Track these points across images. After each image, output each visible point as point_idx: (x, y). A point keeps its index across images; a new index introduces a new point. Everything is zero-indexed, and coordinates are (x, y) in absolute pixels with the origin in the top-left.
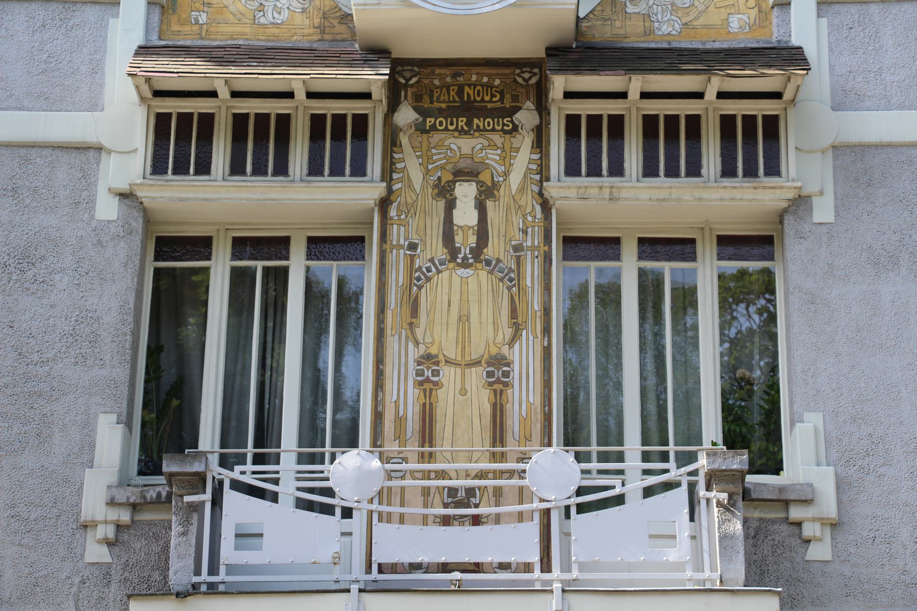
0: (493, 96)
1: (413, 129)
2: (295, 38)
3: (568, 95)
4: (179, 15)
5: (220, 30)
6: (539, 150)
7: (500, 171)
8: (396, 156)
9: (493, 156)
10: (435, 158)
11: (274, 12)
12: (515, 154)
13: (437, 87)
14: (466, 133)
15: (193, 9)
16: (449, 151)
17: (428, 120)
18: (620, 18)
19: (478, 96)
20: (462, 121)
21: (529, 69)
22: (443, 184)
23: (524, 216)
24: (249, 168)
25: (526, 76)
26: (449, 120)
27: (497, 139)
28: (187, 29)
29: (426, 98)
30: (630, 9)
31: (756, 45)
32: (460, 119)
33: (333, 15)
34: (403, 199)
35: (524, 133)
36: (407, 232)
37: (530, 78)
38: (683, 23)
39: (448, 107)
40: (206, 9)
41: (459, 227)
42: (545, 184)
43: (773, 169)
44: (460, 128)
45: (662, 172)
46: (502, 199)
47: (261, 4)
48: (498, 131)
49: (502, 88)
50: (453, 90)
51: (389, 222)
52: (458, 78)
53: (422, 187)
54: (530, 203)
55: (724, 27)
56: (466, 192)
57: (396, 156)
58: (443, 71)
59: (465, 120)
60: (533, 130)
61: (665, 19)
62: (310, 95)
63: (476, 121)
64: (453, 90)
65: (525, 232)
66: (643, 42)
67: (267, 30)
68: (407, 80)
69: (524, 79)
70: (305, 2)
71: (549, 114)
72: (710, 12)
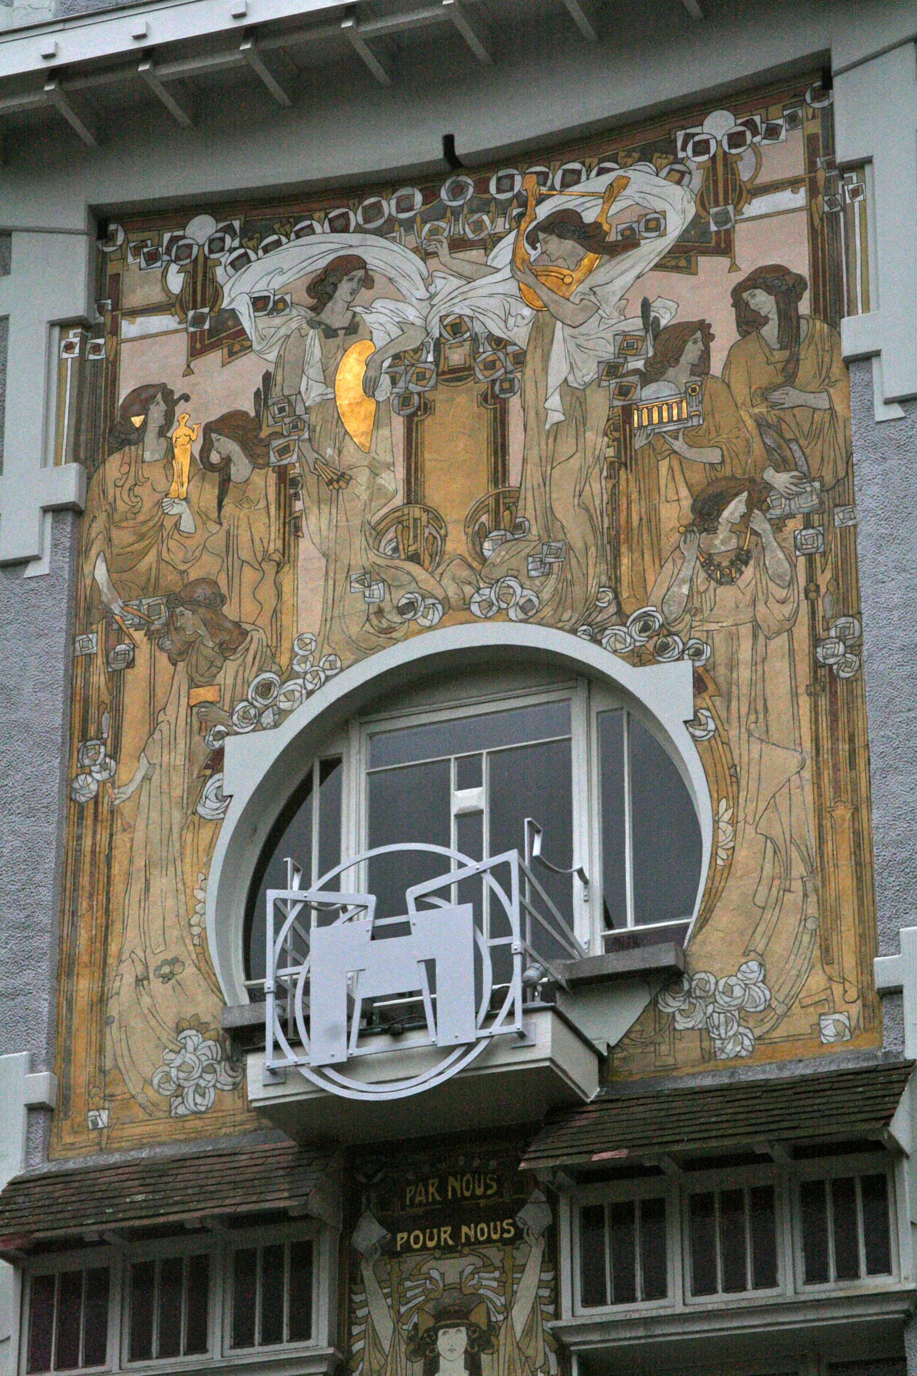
0: (487, 1187)
1: (379, 1253)
2: (224, 1130)
6: (551, 1266)
7: (499, 1304)
8: (357, 1298)
11: (197, 1096)
12: (519, 1275)
15: (91, 1107)
17: (399, 1236)
19: (468, 1189)
20: (445, 1232)
22: (420, 1335)
24: (155, 1348)
28: (82, 1138)
30: (681, 1024)
32: (443, 1229)
34: (366, 1367)
35: (531, 1239)
40: (107, 1105)
46: (502, 1349)
47: (179, 1086)
48: (497, 1241)
59: (449, 1229)
60: (543, 1235)
61: (731, 1033)
63: (465, 1229)
67: (187, 1125)
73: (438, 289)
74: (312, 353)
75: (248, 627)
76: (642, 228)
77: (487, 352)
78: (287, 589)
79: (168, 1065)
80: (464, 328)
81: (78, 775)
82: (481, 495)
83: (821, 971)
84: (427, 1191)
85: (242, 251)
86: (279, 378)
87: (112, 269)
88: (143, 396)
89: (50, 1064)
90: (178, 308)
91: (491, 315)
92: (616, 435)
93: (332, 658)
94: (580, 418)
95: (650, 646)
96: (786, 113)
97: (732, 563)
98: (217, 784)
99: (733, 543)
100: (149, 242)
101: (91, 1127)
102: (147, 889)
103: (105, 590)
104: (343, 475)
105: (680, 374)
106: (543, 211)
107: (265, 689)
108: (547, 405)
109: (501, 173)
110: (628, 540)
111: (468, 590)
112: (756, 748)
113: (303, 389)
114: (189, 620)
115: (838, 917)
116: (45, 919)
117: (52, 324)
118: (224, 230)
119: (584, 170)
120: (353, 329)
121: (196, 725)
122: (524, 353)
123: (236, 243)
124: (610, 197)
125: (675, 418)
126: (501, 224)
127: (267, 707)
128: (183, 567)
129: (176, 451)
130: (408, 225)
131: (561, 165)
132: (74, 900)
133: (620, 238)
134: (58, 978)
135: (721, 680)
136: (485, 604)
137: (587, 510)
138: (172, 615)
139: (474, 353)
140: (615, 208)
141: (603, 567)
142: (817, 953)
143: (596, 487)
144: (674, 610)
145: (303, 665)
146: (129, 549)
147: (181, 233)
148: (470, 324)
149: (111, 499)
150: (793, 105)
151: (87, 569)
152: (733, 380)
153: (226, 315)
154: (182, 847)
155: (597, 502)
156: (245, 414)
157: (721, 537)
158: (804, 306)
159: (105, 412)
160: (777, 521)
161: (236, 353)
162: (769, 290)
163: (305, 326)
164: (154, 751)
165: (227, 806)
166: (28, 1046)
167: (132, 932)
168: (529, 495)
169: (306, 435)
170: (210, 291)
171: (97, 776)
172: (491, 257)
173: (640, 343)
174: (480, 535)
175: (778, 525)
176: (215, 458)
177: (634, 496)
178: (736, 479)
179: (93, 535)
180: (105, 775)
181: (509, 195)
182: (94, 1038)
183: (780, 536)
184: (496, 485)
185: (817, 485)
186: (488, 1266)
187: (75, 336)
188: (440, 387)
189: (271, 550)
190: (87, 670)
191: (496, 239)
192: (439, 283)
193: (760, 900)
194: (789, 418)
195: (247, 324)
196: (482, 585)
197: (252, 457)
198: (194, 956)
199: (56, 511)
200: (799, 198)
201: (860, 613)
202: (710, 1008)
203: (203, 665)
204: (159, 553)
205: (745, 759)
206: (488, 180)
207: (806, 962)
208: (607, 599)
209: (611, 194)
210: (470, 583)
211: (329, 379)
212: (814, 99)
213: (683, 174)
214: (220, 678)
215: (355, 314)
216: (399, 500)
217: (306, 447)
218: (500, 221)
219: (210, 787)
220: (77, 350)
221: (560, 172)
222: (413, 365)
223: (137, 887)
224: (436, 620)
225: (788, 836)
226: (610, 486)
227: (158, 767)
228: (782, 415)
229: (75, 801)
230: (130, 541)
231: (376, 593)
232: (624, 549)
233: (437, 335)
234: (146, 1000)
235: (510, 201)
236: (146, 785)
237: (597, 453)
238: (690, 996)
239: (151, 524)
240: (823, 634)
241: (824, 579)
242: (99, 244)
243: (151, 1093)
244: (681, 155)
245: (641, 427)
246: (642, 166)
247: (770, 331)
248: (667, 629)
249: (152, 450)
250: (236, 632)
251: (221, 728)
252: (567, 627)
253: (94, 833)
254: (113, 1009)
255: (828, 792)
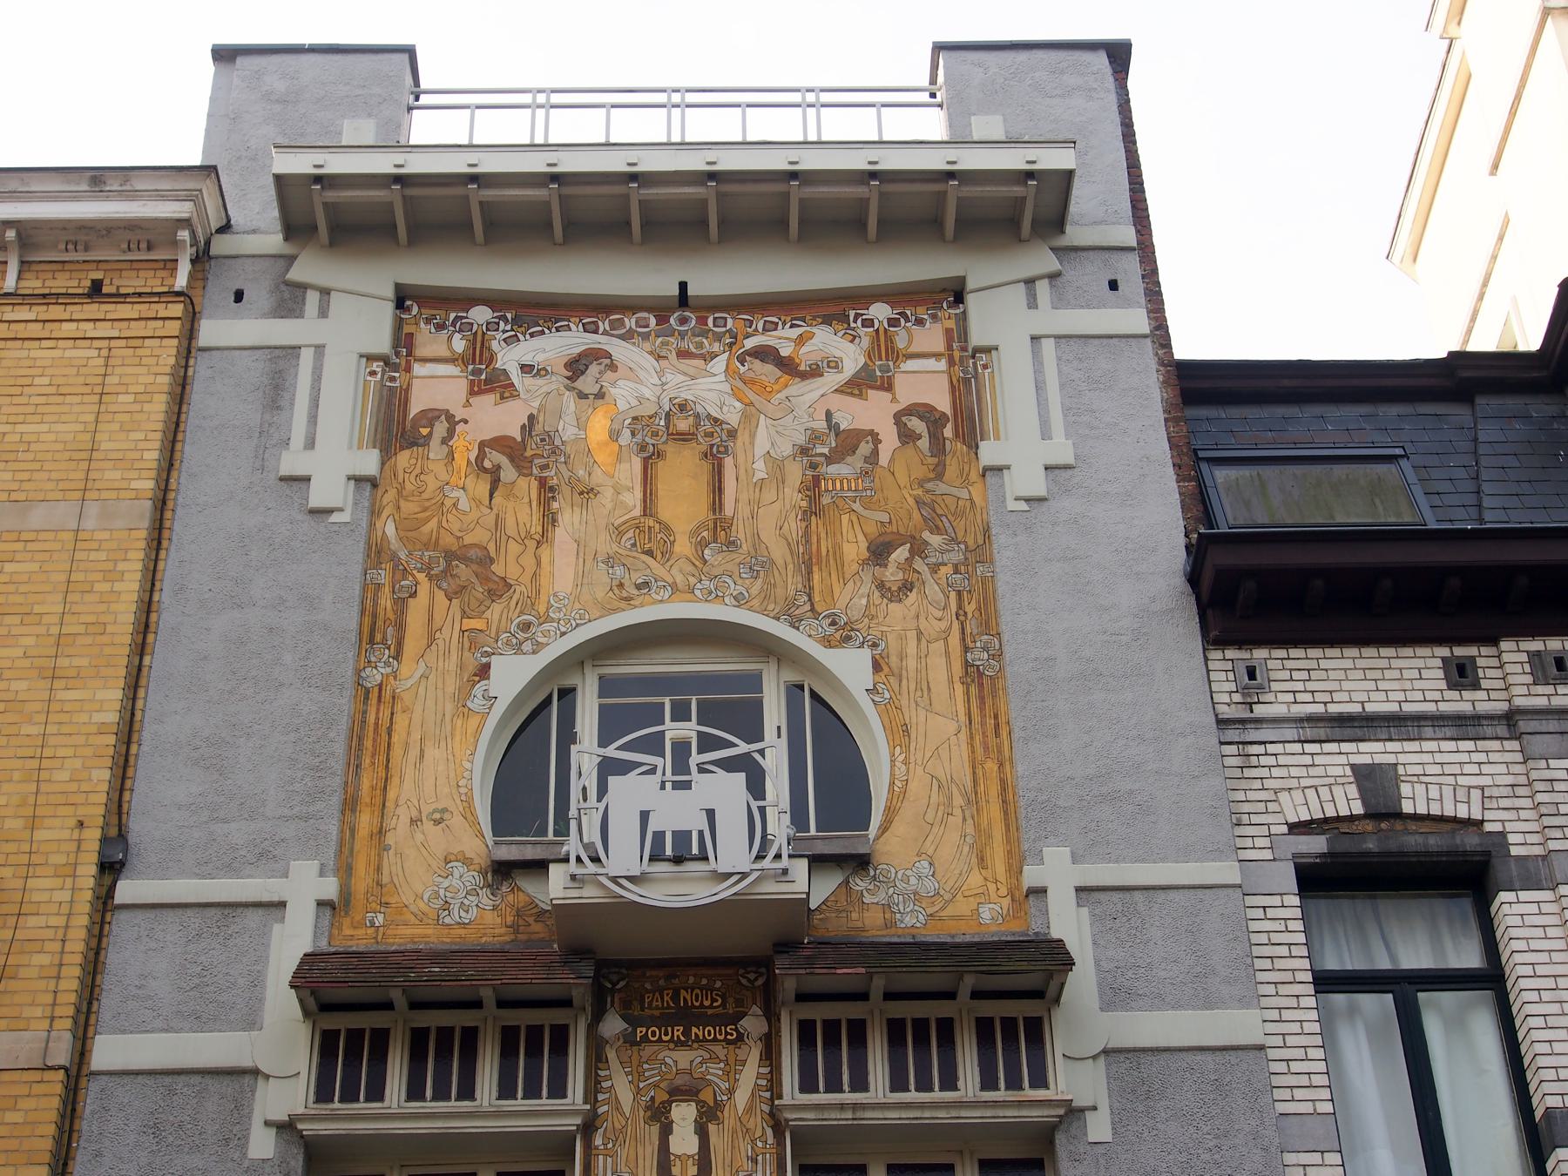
1: (621, 1041)
2: (484, 939)
3: (802, 997)
4: (353, 918)
5: (399, 932)
6: (768, 1062)
8: (602, 1073)
9: (715, 1071)
10: (646, 1074)
12: (741, 1068)
13: (648, 991)
14: (683, 1044)
15: (369, 910)
16: (663, 1066)
18: (857, 909)
19: (697, 1001)
20: (678, 1030)
21: (754, 969)
22: (656, 1105)
23: (753, 1141)
24: (429, 1093)
25: (752, 976)
26: (663, 1029)
27: (719, 1050)
28: (361, 932)
29: (635, 1003)
30: (868, 899)
31: (1009, 939)
32: (676, 1028)
33: (529, 912)
35: (751, 1043)
36: (615, 1164)
37: (756, 979)
38: (928, 913)
39: (660, 1013)
41: (676, 1156)
42: (776, 1102)
43: (1040, 1080)
44: (676, 1038)
45: (912, 1087)
46: (726, 1122)
47: (446, 902)
48: (721, 1041)
49: (723, 990)
50: (667, 995)
51: (594, 1152)
52: (673, 981)
53: (632, 1108)
54: (758, 1124)
55: (974, 918)
56: (684, 1115)
57: (599, 1071)
58: (654, 973)
59: (682, 1028)
60: (760, 1039)
62: (502, 1004)
63: (694, 1030)
64: (667, 995)
65: (755, 1162)
66: (883, 936)
67: (451, 931)
68: (614, 985)
69: (749, 980)
70: (497, 899)
71: (779, 1020)
72: (958, 901)
73: (668, 380)
74: (568, 407)
75: (512, 582)
76: (825, 365)
77: (707, 426)
78: (545, 559)
79: (437, 886)
80: (688, 409)
81: (364, 668)
82: (702, 518)
83: (978, 873)
84: (662, 999)
85: (513, 333)
86: (541, 419)
87: (407, 329)
88: (430, 415)
89: (337, 872)
90: (460, 361)
91: (707, 401)
92: (808, 493)
93: (582, 611)
94: (780, 478)
95: (838, 635)
96: (929, 312)
97: (900, 588)
98: (484, 688)
99: (900, 576)
100: (438, 317)
101: (368, 924)
102: (422, 756)
103: (393, 541)
104: (592, 489)
105: (855, 464)
106: (750, 343)
107: (526, 626)
108: (754, 466)
109: (716, 315)
110: (819, 563)
111: (693, 580)
112: (922, 713)
113: (560, 429)
114: (463, 571)
115: (990, 836)
116: (338, 765)
117: (361, 356)
118: (499, 318)
119: (780, 323)
120: (600, 395)
121: (467, 645)
122: (736, 431)
123: (509, 327)
124: (799, 343)
125: (853, 489)
126: (716, 347)
127: (527, 639)
128: (459, 534)
129: (455, 455)
130: (646, 337)
131: (763, 317)
132: (358, 757)
133: (808, 369)
134: (343, 813)
135: (893, 665)
136: (705, 591)
137: (787, 540)
138: (449, 565)
139: (697, 425)
140: (804, 350)
141: (800, 579)
142: (974, 860)
143: (793, 525)
144: (855, 614)
145: (558, 614)
146: (415, 516)
147: (465, 315)
148: (693, 406)
149: (401, 480)
150: (934, 308)
151: (379, 525)
152: (895, 470)
153: (499, 372)
154: (453, 729)
155: (794, 536)
156: (514, 439)
157: (891, 571)
158: (948, 432)
159: (398, 422)
160: (933, 566)
161: (507, 398)
162: (921, 418)
163: (562, 388)
164: (431, 657)
165: (492, 705)
166: (318, 858)
167: (408, 784)
168: (741, 522)
169: (563, 460)
170: (486, 355)
171: (382, 670)
172: (710, 365)
173: (825, 438)
174: (703, 544)
175: (934, 569)
176: (487, 464)
177: (823, 535)
178: (903, 535)
179: (385, 502)
180: (389, 670)
181: (724, 329)
182: (372, 859)
183: (935, 576)
184: (714, 513)
185: (962, 546)
186: (714, 1058)
187: (377, 366)
188: (669, 442)
189: (533, 531)
190: (375, 596)
191: (714, 356)
192: (669, 377)
193: (930, 817)
194: (939, 500)
195: (515, 380)
196: (703, 578)
197: (518, 467)
198: (461, 809)
199: (358, 480)
200: (942, 365)
201: (999, 634)
202: (891, 890)
203: (474, 603)
204: (440, 522)
205: (914, 721)
206: (707, 318)
207: (967, 865)
208: (803, 600)
209: (801, 340)
210: (694, 575)
211: (581, 425)
212: (948, 308)
213: (855, 337)
214: (488, 614)
215: (602, 386)
216: (637, 512)
217: (562, 468)
218: (717, 344)
219: (479, 689)
220: (379, 376)
221: (762, 322)
222: (648, 426)
223: (414, 752)
224: (666, 597)
225: (949, 777)
226: (804, 526)
227: (434, 670)
228: (934, 498)
229: (362, 686)
230: (416, 510)
231: (618, 572)
232: (815, 569)
233: (668, 409)
234: (419, 837)
235: (725, 333)
236: (425, 680)
237: (793, 504)
238: (875, 880)
239: (434, 501)
240: (971, 645)
241: (970, 608)
242: (398, 312)
243: (422, 906)
244: (853, 325)
245: (827, 490)
246: (823, 327)
247: (924, 443)
248: (850, 626)
249: (436, 450)
250: (502, 584)
251: (486, 649)
252: (772, 615)
253: (378, 710)
254: (390, 839)
255: (979, 750)
